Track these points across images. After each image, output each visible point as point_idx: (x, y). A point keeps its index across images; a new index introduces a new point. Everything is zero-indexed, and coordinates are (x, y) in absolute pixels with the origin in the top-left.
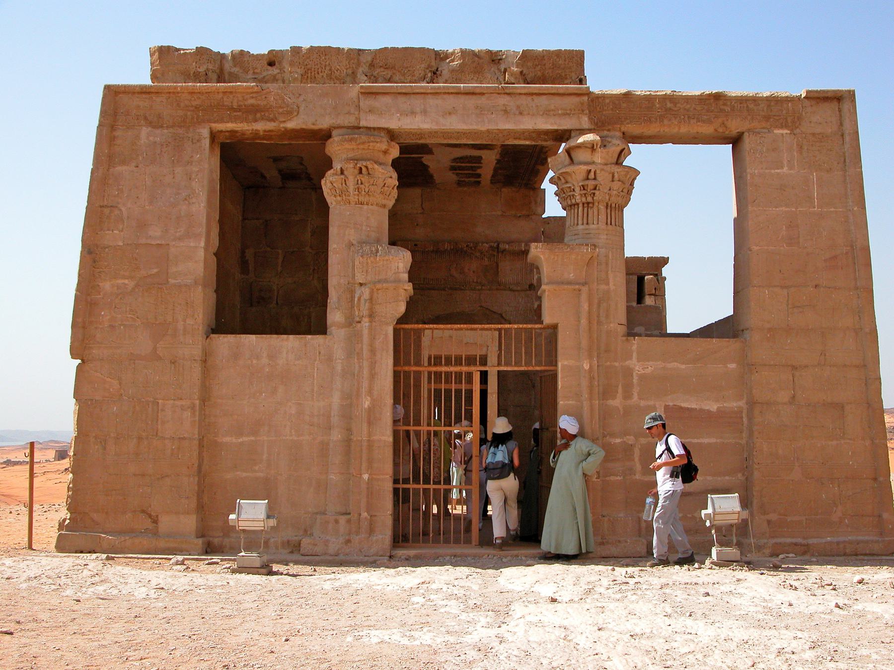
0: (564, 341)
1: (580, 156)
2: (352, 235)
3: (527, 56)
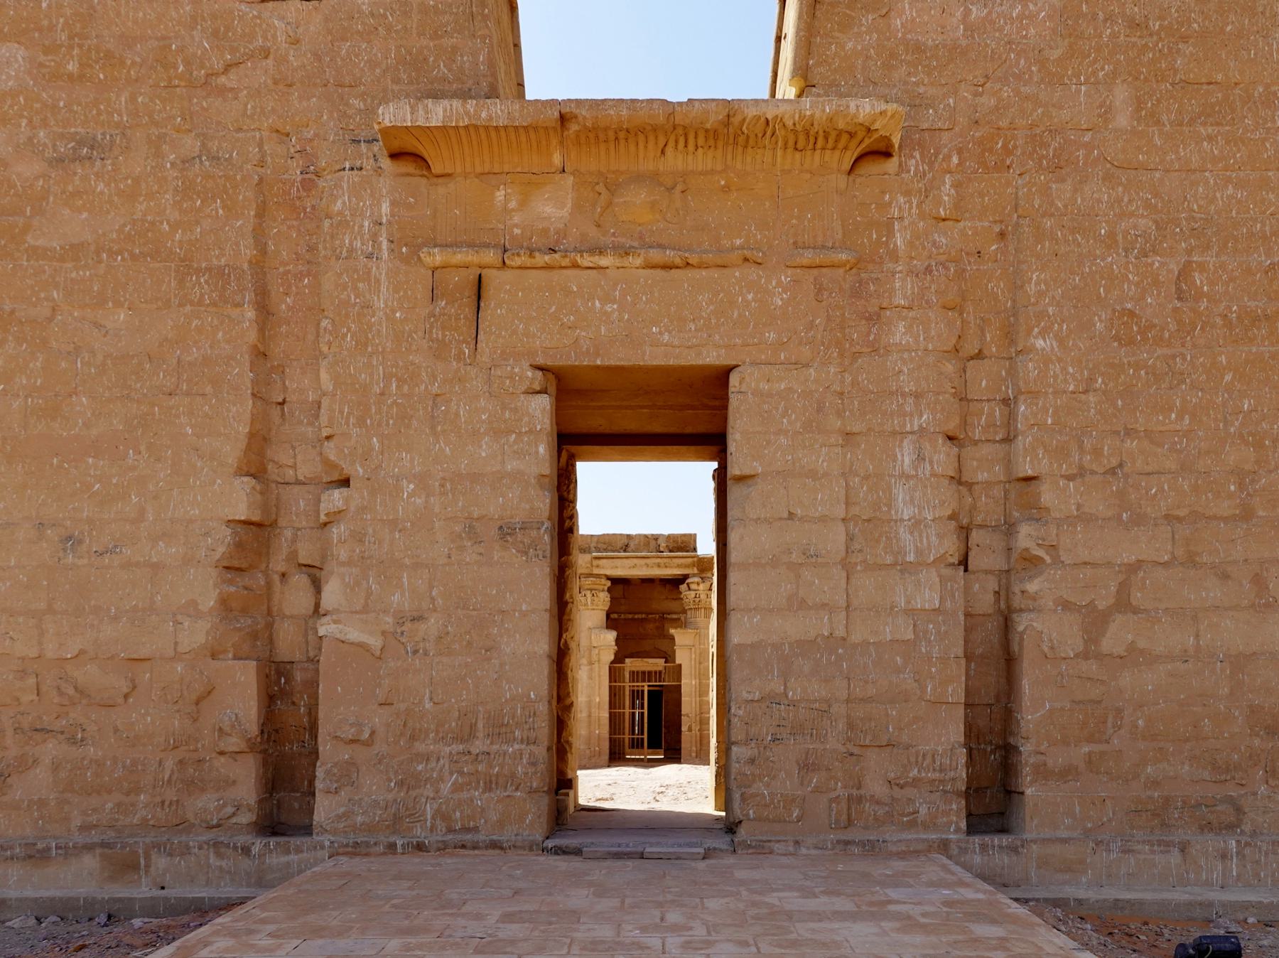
0: (685, 671)
1: (693, 586)
2: (589, 624)
3: (669, 536)
